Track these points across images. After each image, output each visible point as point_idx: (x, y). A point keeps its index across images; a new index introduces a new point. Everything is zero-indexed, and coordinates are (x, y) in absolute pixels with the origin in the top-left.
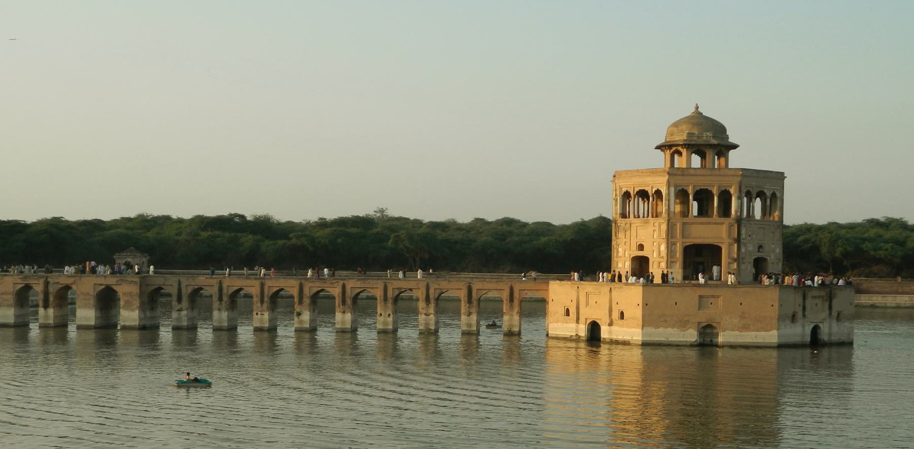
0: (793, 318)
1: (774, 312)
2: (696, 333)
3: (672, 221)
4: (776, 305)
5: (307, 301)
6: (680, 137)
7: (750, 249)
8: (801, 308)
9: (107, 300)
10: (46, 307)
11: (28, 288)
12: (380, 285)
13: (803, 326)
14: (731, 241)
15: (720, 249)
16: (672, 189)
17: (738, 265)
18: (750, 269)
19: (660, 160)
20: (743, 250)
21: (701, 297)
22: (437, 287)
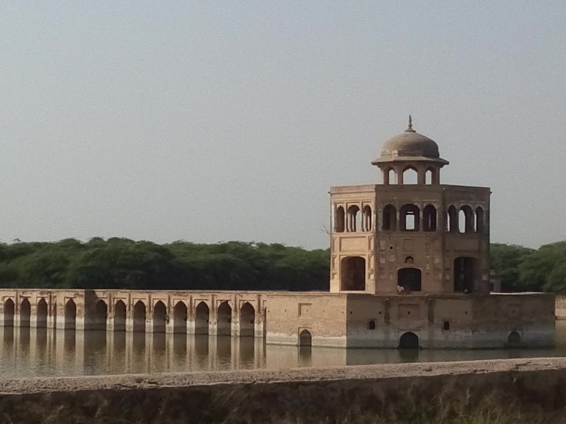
0: (372, 325)
1: (343, 319)
2: (297, 337)
3: (333, 236)
4: (345, 312)
5: (172, 310)
6: (394, 156)
7: (392, 260)
8: (383, 314)
9: (71, 308)
10: (50, 315)
11: (43, 299)
12: (210, 298)
13: (387, 333)
14: (370, 253)
15: (364, 260)
16: (333, 207)
17: (376, 275)
18: (394, 278)
19: (378, 177)
20: (383, 261)
21: (300, 305)
22: (241, 299)
